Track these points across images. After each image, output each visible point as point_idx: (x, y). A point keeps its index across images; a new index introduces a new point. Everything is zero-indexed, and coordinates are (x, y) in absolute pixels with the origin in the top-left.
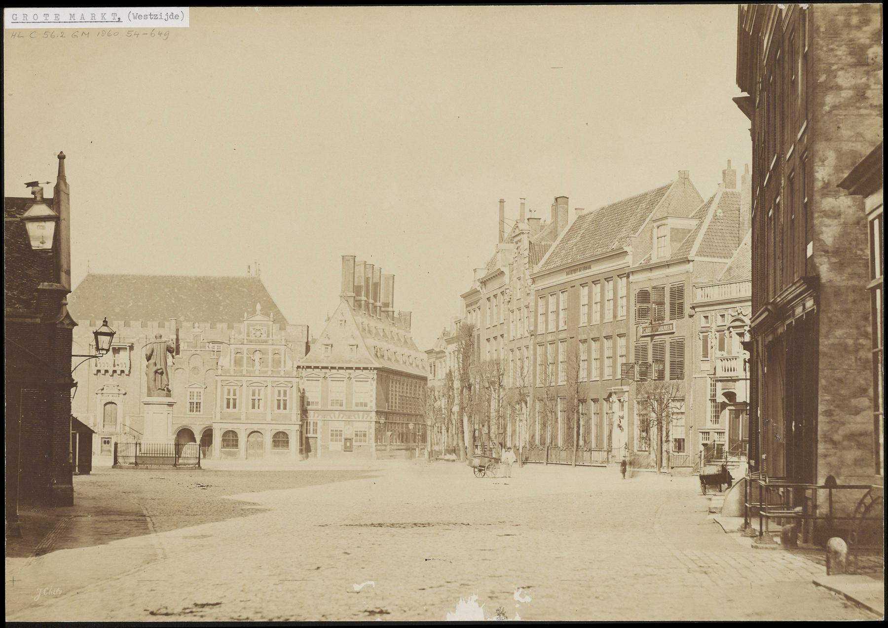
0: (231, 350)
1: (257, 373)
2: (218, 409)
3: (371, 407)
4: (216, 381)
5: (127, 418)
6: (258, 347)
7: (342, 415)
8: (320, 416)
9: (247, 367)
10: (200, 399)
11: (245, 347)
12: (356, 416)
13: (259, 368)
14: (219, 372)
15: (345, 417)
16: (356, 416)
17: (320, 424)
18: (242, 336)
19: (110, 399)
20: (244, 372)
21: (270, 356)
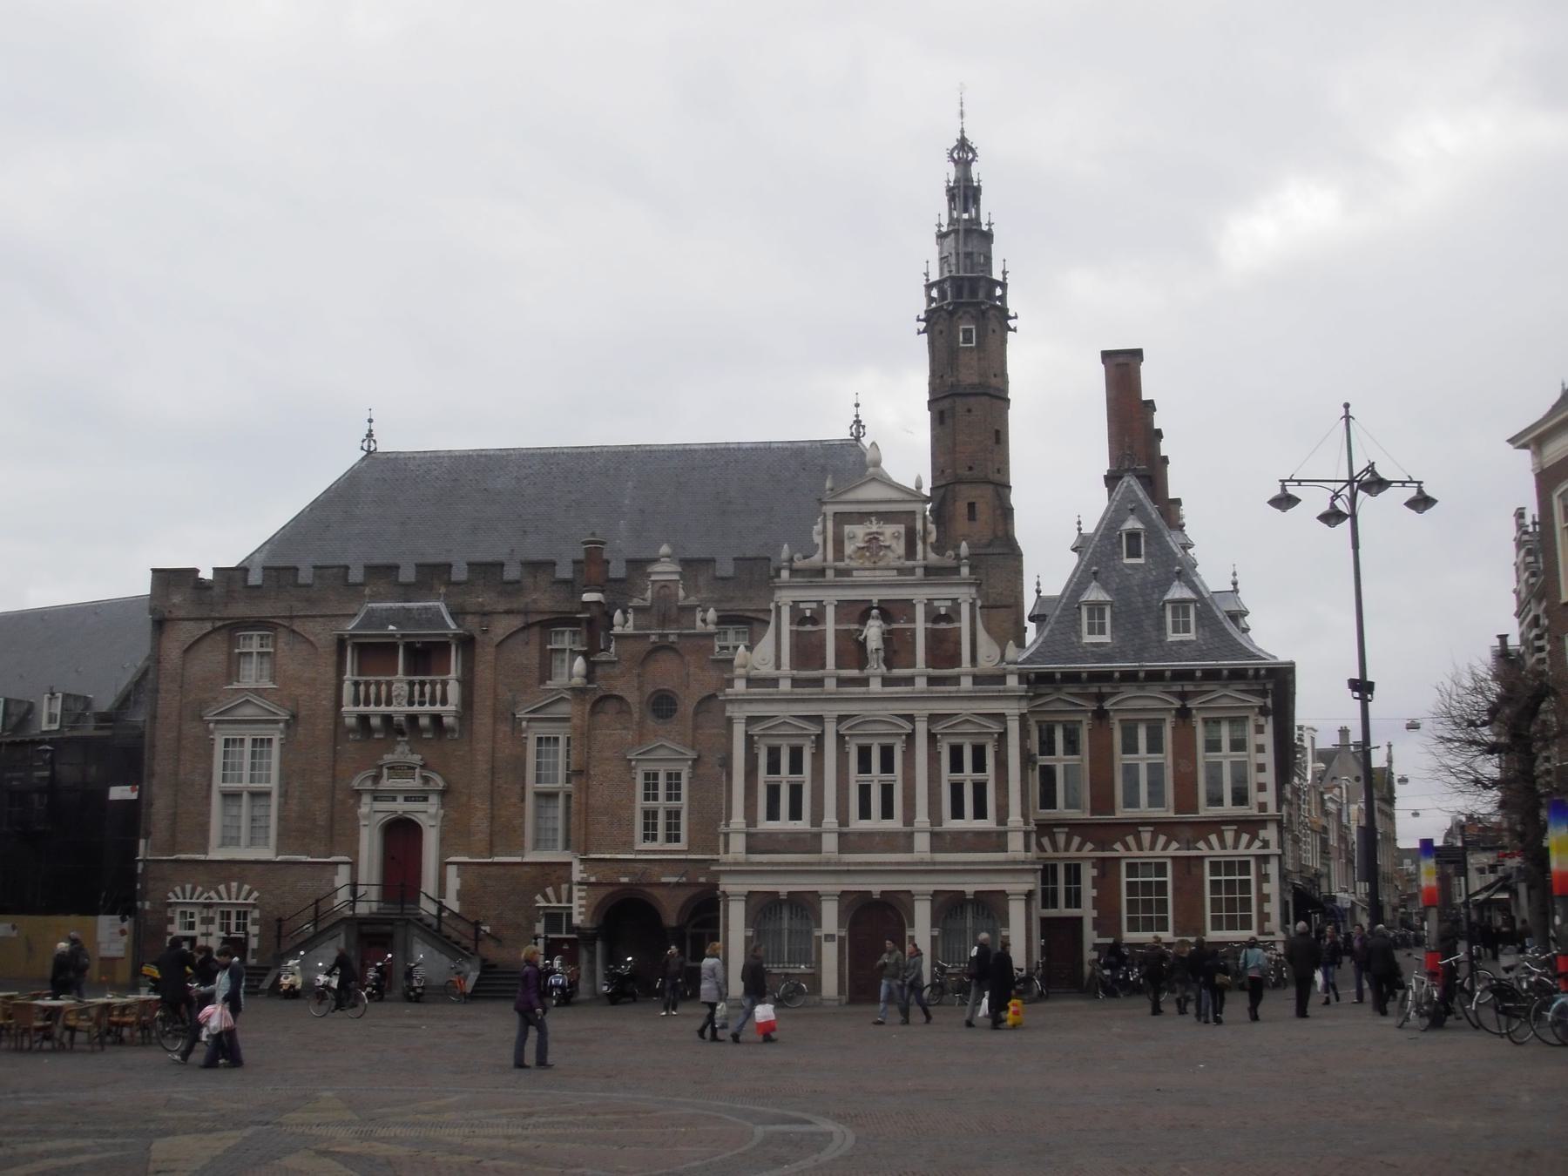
0: (778, 609)
1: (875, 686)
2: (738, 820)
3: (1263, 807)
4: (730, 721)
5: (452, 872)
6: (875, 595)
7: (1162, 839)
8: (1089, 846)
9: (839, 666)
10: (678, 798)
11: (830, 597)
12: (1213, 838)
13: (884, 669)
14: (740, 686)
15: (1175, 845)
16: (1213, 838)
17: (1088, 873)
18: (817, 558)
19: (400, 807)
20: (831, 685)
21: (920, 626)
